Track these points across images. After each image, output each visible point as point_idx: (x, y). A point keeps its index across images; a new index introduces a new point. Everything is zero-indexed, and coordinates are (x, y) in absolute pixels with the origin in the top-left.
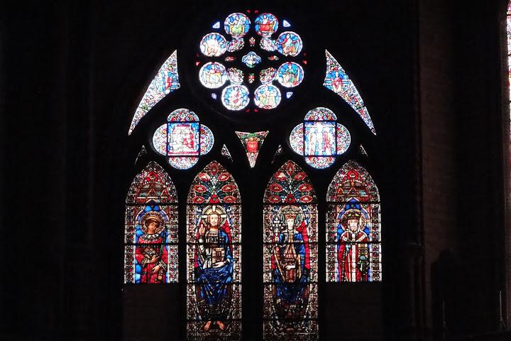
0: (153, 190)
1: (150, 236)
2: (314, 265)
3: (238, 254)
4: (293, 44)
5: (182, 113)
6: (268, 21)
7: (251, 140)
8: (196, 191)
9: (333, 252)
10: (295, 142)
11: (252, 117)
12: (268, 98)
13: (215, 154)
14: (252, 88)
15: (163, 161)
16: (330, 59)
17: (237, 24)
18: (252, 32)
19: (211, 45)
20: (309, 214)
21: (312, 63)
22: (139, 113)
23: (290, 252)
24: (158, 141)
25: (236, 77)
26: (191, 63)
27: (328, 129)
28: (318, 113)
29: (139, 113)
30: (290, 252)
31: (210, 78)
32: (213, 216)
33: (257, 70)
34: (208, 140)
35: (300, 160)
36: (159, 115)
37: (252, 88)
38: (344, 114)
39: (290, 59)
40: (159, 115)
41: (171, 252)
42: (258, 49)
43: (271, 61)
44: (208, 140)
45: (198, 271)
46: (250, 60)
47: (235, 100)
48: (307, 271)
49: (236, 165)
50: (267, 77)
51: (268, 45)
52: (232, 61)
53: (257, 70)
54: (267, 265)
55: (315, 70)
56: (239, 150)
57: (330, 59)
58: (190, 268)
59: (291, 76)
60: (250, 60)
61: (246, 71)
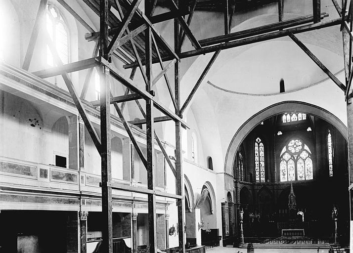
4: (300, 143)
7: (295, 157)
10: (301, 156)
11: (295, 153)
12: (298, 150)
19: (290, 145)
21: (303, 146)
22: (281, 154)
24: (284, 157)
29: (281, 154)
32: (291, 166)
36: (284, 154)
40: (284, 154)
47: (293, 151)
49: (294, 160)
56: (294, 158)
60: (295, 146)
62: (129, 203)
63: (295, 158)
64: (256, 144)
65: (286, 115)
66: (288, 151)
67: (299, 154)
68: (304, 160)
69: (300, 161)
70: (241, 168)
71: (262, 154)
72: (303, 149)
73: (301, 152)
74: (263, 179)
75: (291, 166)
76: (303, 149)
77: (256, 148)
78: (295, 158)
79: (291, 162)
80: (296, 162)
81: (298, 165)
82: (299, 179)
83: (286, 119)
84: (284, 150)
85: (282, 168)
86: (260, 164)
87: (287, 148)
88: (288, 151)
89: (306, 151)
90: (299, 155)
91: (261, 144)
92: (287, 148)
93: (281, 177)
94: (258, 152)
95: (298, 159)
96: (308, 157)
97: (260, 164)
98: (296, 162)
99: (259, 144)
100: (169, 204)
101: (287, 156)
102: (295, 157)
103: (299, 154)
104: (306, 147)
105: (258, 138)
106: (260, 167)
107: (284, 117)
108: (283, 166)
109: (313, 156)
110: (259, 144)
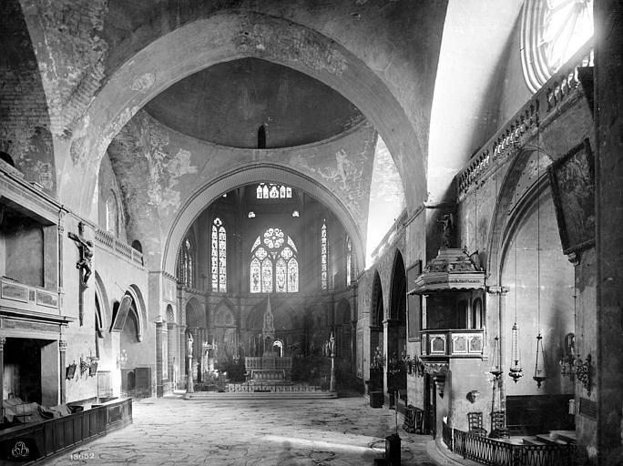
1: (255, 272)
11: (274, 249)
13: (267, 257)
19: (266, 234)
21: (286, 239)
24: (257, 254)
38: (292, 249)
40: (256, 249)
43: (277, 238)
44: (266, 254)
46: (274, 238)
47: (271, 246)
49: (271, 259)
55: (286, 239)
56: (272, 256)
59: (282, 241)
60: (274, 238)
62: (56, 325)
64: (214, 229)
65: (262, 187)
66: (263, 245)
69: (281, 262)
70: (188, 266)
71: (223, 245)
72: (285, 245)
73: (282, 248)
74: (223, 287)
76: (285, 245)
77: (214, 235)
79: (268, 262)
80: (274, 263)
81: (278, 268)
82: (278, 290)
83: (263, 192)
84: (258, 242)
85: (252, 272)
86: (219, 261)
87: (262, 240)
88: (263, 245)
89: (292, 249)
91: (222, 229)
92: (262, 240)
93: (252, 284)
94: (216, 242)
95: (277, 259)
96: (293, 257)
97: (219, 261)
98: (274, 263)
99: (218, 228)
100: (67, 322)
101: (261, 253)
104: (290, 242)
105: (218, 219)
107: (259, 189)
108: (254, 268)
109: (298, 256)
110: (218, 228)
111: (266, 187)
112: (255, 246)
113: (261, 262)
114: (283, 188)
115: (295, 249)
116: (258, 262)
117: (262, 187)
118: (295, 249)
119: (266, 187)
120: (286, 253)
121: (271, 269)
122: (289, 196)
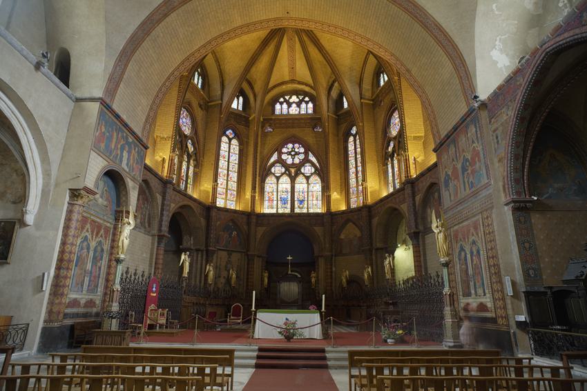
0: (271, 180)
1: (271, 190)
2: (306, 196)
3: (290, 194)
4: (302, 150)
5: (278, 165)
6: (297, 145)
7: (293, 171)
8: (281, 181)
9: (310, 194)
10: (302, 170)
11: (293, 165)
12: (297, 161)
14: (293, 159)
15: (274, 174)
16: (310, 153)
17: (290, 146)
18: (293, 147)
19: (284, 150)
20: (306, 185)
21: (306, 153)
23: (301, 194)
24: (273, 170)
25: (290, 157)
26: (280, 154)
27: (310, 168)
28: (307, 165)
30: (301, 194)
31: (284, 157)
32: (284, 186)
33: (294, 155)
34: (283, 170)
35: (303, 174)
37: (293, 159)
38: (313, 165)
39: (300, 153)
40: (273, 165)
41: (275, 193)
42: (294, 151)
45: (281, 198)
46: (293, 153)
47: (290, 161)
48: (305, 198)
49: (290, 175)
50: (297, 156)
51: (297, 150)
52: (289, 153)
53: (294, 155)
54: (296, 196)
57: (310, 153)
58: (279, 197)
59: (302, 157)
60: (293, 153)
61: (292, 156)
63: (293, 172)
64: (224, 139)
65: (281, 103)
66: (281, 161)
67: (298, 167)
68: (307, 178)
69: (300, 179)
71: (235, 158)
73: (303, 163)
75: (284, 186)
77: (224, 146)
78: (293, 172)
79: (285, 180)
81: (297, 186)
82: (297, 211)
84: (274, 157)
88: (281, 161)
90: (300, 170)
91: (235, 142)
95: (297, 174)
96: (315, 171)
99: (230, 140)
101: (278, 169)
102: (293, 171)
103: (298, 167)
104: (314, 160)
105: (230, 131)
106: (227, 181)
107: (278, 106)
108: (270, 183)
111: (285, 104)
112: (272, 160)
113: (278, 178)
114: (303, 105)
115: (318, 165)
116: (274, 180)
117: (281, 103)
118: (318, 165)
119: (285, 104)
120: (308, 169)
121: (289, 187)
122: (310, 111)
